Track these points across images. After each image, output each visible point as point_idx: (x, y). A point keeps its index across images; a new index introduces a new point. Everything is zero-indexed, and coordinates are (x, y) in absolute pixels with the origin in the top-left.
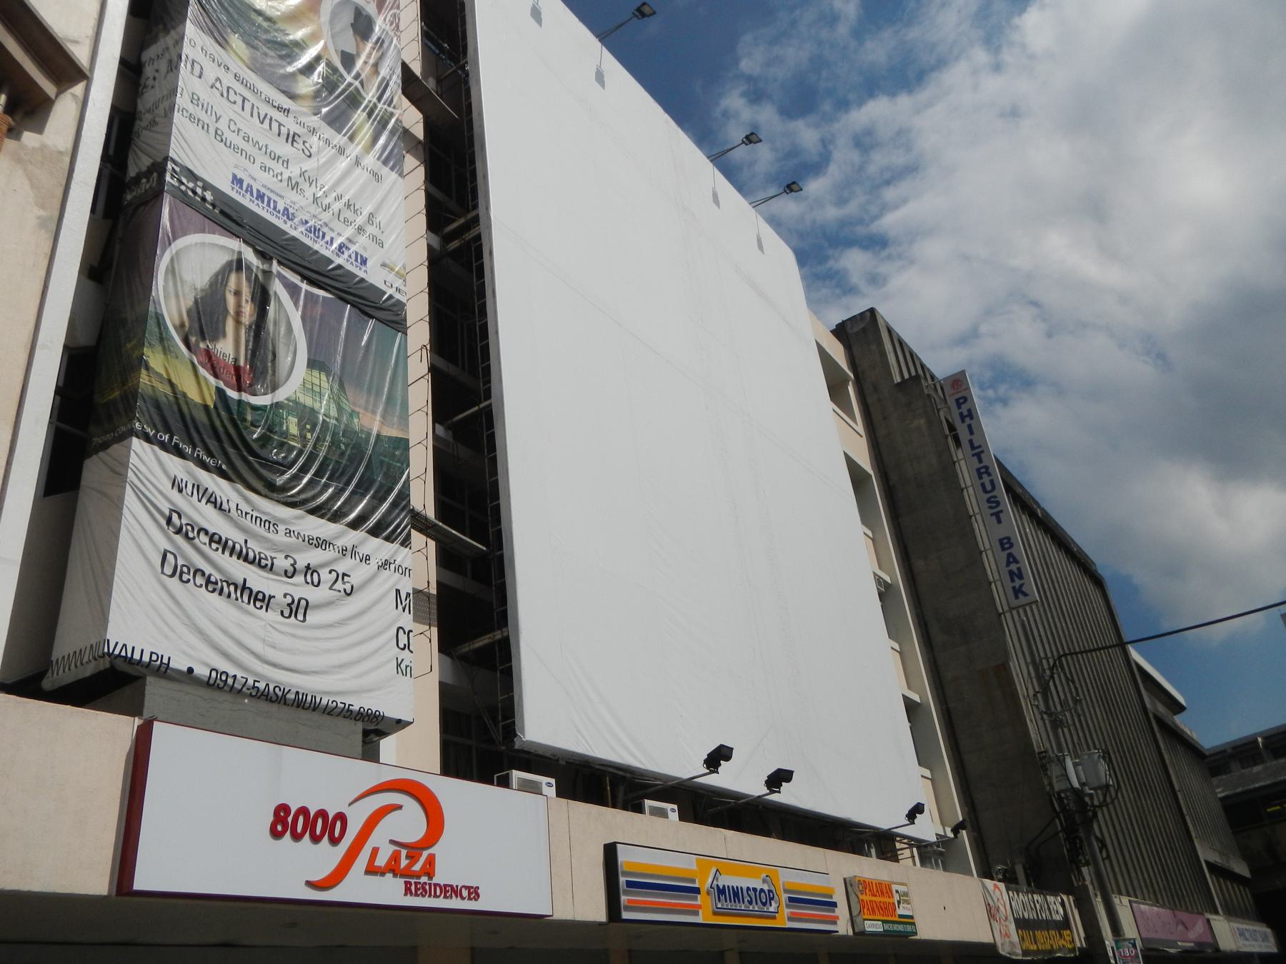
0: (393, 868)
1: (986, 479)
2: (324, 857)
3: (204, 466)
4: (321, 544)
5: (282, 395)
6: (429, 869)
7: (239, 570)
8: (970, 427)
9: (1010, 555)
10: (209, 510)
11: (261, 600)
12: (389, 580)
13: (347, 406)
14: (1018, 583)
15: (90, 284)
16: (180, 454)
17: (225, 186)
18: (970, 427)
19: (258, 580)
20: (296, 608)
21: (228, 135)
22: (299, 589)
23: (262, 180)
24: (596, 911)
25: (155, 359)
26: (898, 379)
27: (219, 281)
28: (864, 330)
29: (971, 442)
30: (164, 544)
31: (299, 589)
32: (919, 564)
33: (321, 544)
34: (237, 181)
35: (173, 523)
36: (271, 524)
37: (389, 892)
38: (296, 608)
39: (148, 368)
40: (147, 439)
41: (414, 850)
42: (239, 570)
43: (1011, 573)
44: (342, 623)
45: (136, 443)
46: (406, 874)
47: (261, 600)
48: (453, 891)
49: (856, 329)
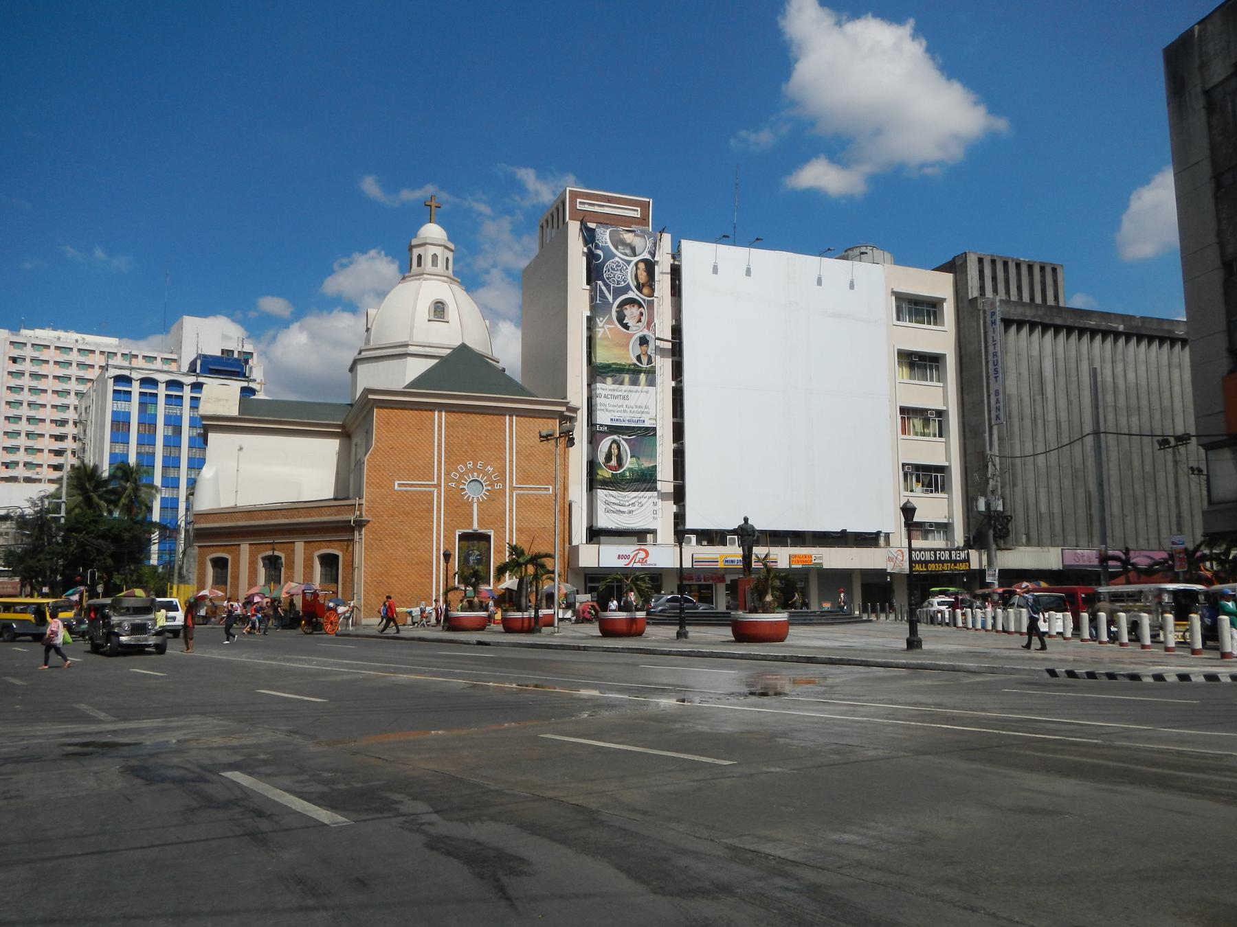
0: (639, 562)
1: (995, 359)
2: (627, 561)
3: (610, 490)
4: (635, 497)
5: (624, 468)
6: (646, 561)
7: (618, 508)
8: (994, 329)
9: (997, 399)
10: (612, 498)
11: (623, 512)
12: (651, 500)
13: (640, 463)
14: (998, 413)
15: (590, 445)
16: (606, 489)
17: (609, 423)
18: (994, 329)
19: (622, 509)
20: (630, 512)
21: (609, 408)
22: (631, 508)
23: (616, 415)
24: (691, 567)
25: (600, 472)
26: (970, 298)
27: (611, 446)
28: (962, 264)
29: (993, 337)
30: (605, 507)
31: (631, 508)
32: (966, 397)
33: (635, 497)
34: (612, 420)
35: (607, 503)
36: (625, 497)
37: (637, 565)
38: (630, 512)
39: (598, 474)
40: (599, 488)
41: (643, 559)
42: (618, 508)
43: (997, 407)
44: (640, 512)
45: (599, 490)
46: (642, 562)
47: (623, 512)
48: (649, 565)
49: (960, 262)
